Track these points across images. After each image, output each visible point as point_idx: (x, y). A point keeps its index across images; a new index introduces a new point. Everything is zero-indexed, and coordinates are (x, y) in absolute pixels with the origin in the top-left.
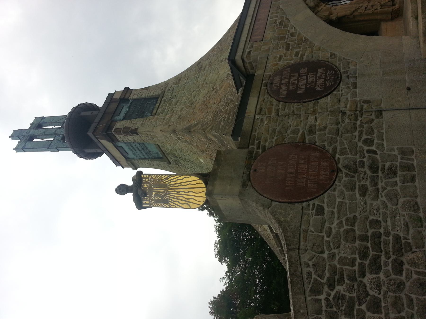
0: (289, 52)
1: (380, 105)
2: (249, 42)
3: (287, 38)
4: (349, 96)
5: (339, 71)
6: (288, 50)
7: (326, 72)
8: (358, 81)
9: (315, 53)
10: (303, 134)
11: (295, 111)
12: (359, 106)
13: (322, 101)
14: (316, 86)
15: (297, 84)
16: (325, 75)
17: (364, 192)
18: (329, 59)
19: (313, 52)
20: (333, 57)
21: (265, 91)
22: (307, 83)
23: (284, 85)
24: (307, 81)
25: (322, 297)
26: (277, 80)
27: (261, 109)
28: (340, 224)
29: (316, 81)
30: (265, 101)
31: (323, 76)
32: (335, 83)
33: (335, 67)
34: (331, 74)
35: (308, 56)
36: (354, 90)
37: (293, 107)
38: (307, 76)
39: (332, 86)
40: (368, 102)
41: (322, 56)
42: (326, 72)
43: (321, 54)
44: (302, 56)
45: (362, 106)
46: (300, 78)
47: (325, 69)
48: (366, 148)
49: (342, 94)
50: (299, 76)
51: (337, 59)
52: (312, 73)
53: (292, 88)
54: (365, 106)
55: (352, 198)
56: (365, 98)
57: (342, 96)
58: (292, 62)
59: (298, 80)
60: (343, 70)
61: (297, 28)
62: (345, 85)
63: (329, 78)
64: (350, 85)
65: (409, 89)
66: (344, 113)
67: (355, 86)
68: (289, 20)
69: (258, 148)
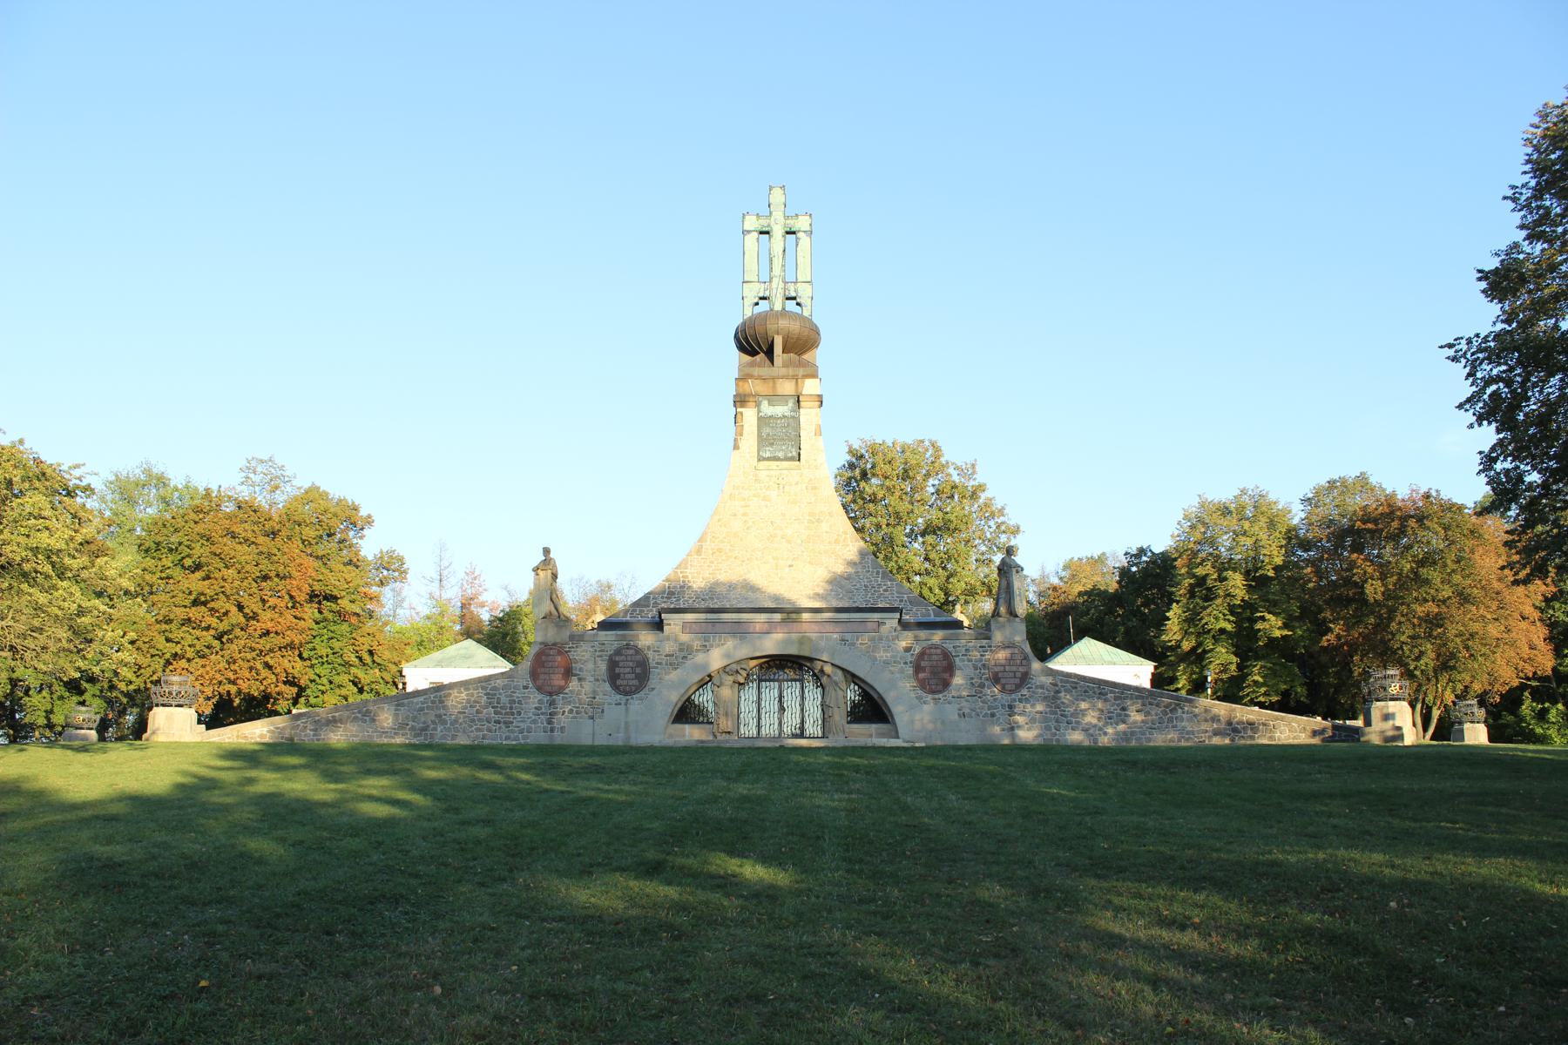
8: (623, 707)
26: (631, 652)
41: (653, 682)
55: (534, 703)
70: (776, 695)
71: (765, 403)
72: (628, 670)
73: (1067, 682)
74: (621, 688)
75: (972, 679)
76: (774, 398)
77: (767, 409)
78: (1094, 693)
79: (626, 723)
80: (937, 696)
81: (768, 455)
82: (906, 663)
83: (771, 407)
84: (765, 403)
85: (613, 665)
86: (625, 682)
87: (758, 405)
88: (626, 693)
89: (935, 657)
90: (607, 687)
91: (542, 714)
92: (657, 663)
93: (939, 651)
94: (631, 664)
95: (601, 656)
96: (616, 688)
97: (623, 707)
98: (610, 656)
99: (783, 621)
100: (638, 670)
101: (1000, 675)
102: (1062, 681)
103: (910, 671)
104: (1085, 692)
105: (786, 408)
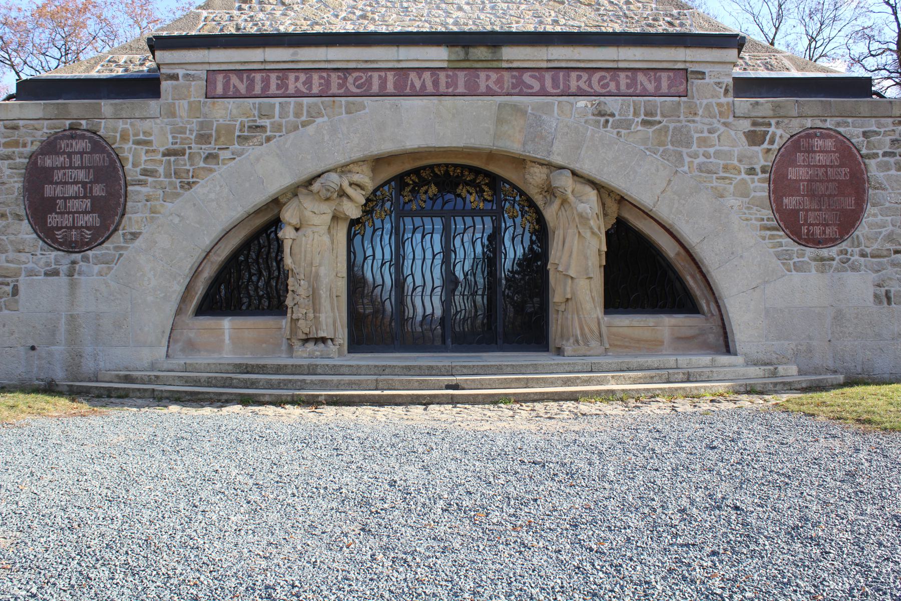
0: (159, 157)
1: (6, 309)
2: (207, 71)
3: (203, 147)
4: (30, 265)
5: (90, 249)
6: (164, 155)
7: (88, 228)
8: (63, 279)
9: (146, 205)
11: (7, 186)
12: (9, 280)
13: (25, 225)
14: (57, 213)
15: (66, 183)
16: (82, 227)
18: (123, 229)
19: (147, 201)
20: (129, 237)
21: (60, 128)
22: (65, 199)
23: (67, 160)
24: (71, 198)
26: (80, 145)
27: (15, 128)
29: (69, 213)
30: (35, 131)
31: (81, 223)
32: (61, 244)
33: (99, 242)
34: (82, 235)
35: (139, 192)
36: (43, 273)
37: (16, 182)
38: (85, 197)
39: (55, 240)
40: (15, 292)
42: (88, 228)
43: (141, 215)
44: (140, 183)
45: (8, 284)
46: (80, 185)
47: (98, 225)
49: (36, 255)
50: (84, 184)
51: (122, 245)
52: (89, 204)
53: (58, 175)
56: (22, 288)
57: (32, 255)
58: (129, 166)
59: (76, 183)
60: (91, 255)
61: (232, 163)
62: (55, 259)
63: (74, 233)
64: (54, 266)
65: (33, 348)
68: (265, 145)
70: (438, 248)
72: (72, 190)
74: (59, 234)
79: (72, 318)
80: (825, 252)
82: (751, 171)
86: (67, 221)
88: (71, 246)
89: (819, 158)
90: (25, 231)
92: (145, 172)
93: (829, 144)
97: (63, 279)
98: (32, 156)
99: (453, 68)
100: (98, 190)
103: (760, 188)
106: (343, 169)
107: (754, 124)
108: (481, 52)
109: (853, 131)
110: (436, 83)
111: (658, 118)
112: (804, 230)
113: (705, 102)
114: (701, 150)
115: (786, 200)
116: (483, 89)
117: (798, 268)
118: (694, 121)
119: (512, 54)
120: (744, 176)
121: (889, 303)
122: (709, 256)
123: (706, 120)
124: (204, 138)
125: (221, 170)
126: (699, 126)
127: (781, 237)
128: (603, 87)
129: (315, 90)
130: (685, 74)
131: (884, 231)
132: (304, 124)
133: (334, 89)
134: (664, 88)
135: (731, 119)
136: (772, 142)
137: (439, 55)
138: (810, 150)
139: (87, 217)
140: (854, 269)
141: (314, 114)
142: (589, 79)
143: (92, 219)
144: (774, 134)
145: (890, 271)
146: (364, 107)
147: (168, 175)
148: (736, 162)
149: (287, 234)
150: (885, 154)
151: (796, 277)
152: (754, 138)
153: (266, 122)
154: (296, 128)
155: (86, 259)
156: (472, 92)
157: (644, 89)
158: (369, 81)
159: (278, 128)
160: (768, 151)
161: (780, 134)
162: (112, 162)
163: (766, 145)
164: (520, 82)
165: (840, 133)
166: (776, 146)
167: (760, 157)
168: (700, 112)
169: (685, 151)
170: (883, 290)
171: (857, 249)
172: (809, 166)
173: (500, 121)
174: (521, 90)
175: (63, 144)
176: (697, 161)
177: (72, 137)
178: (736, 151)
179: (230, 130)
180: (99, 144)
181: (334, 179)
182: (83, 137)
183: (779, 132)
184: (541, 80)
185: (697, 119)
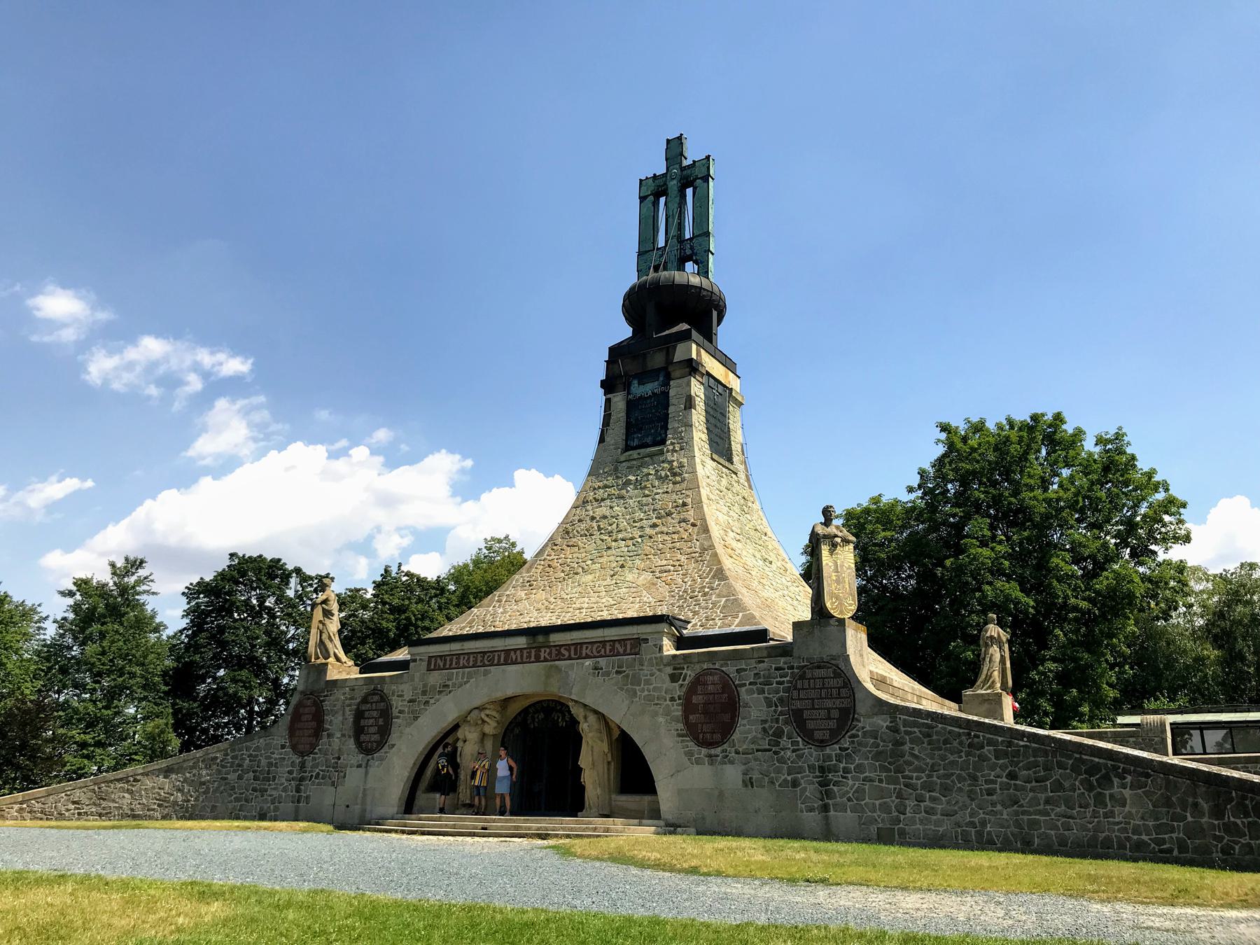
0: (406, 703)
8: (362, 770)
10: (328, 729)
17: (290, 772)
25: (245, 752)
26: (376, 698)
28: (276, 759)
31: (373, 739)
40: (345, 777)
41: (394, 738)
44: (398, 717)
48: (314, 774)
53: (367, 714)
54: (342, 774)
58: (394, 709)
61: (434, 706)
65: (348, 806)
66: (339, 758)
67: (359, 766)
69: (324, 696)
71: (635, 382)
73: (915, 724)
75: (765, 722)
76: (644, 377)
77: (638, 390)
78: (961, 743)
80: (713, 752)
81: (636, 443)
82: (672, 699)
83: (641, 387)
84: (635, 382)
85: (359, 715)
87: (627, 387)
89: (710, 688)
90: (351, 744)
91: (293, 779)
92: (400, 712)
93: (716, 678)
94: (375, 714)
95: (349, 705)
96: (359, 744)
101: (806, 714)
102: (906, 724)
103: (677, 711)
104: (946, 742)
105: (656, 383)
106: (480, 708)
107: (675, 669)
108: (540, 638)
109: (731, 669)
110: (522, 656)
111: (624, 669)
112: (701, 736)
113: (648, 657)
114: (646, 687)
115: (691, 717)
116: (542, 659)
117: (698, 762)
118: (642, 670)
119: (556, 638)
120: (668, 702)
121: (752, 787)
122: (648, 753)
123: (649, 668)
124: (424, 693)
125: (431, 709)
126: (646, 672)
127: (687, 741)
128: (598, 652)
129: (471, 665)
130: (638, 642)
131: (750, 737)
132: (466, 683)
133: (479, 664)
134: (628, 651)
135: (662, 667)
136: (684, 680)
137: (521, 642)
138: (705, 684)
139: (376, 736)
140: (732, 763)
141: (470, 676)
142: (592, 649)
143: (377, 737)
144: (686, 674)
145: (753, 764)
146: (490, 673)
147: (408, 713)
148: (663, 694)
149: (460, 744)
150: (750, 684)
151: (696, 768)
152: (674, 678)
153: (450, 683)
154: (461, 685)
155: (373, 759)
156: (538, 660)
157: (618, 652)
158: (494, 657)
159: (454, 685)
160: (682, 685)
161: (690, 673)
162: (387, 708)
163: (680, 682)
164: (559, 653)
165: (723, 671)
166: (686, 682)
167: (678, 690)
168: (646, 663)
169: (637, 688)
170: (748, 777)
171: (733, 749)
172: (705, 694)
173: (548, 676)
174: (560, 657)
175: (370, 697)
176: (643, 694)
177: (374, 694)
178: (665, 686)
179: (434, 687)
180: (384, 698)
181: (475, 714)
182: (377, 694)
183: (689, 673)
184: (569, 651)
185: (644, 668)
